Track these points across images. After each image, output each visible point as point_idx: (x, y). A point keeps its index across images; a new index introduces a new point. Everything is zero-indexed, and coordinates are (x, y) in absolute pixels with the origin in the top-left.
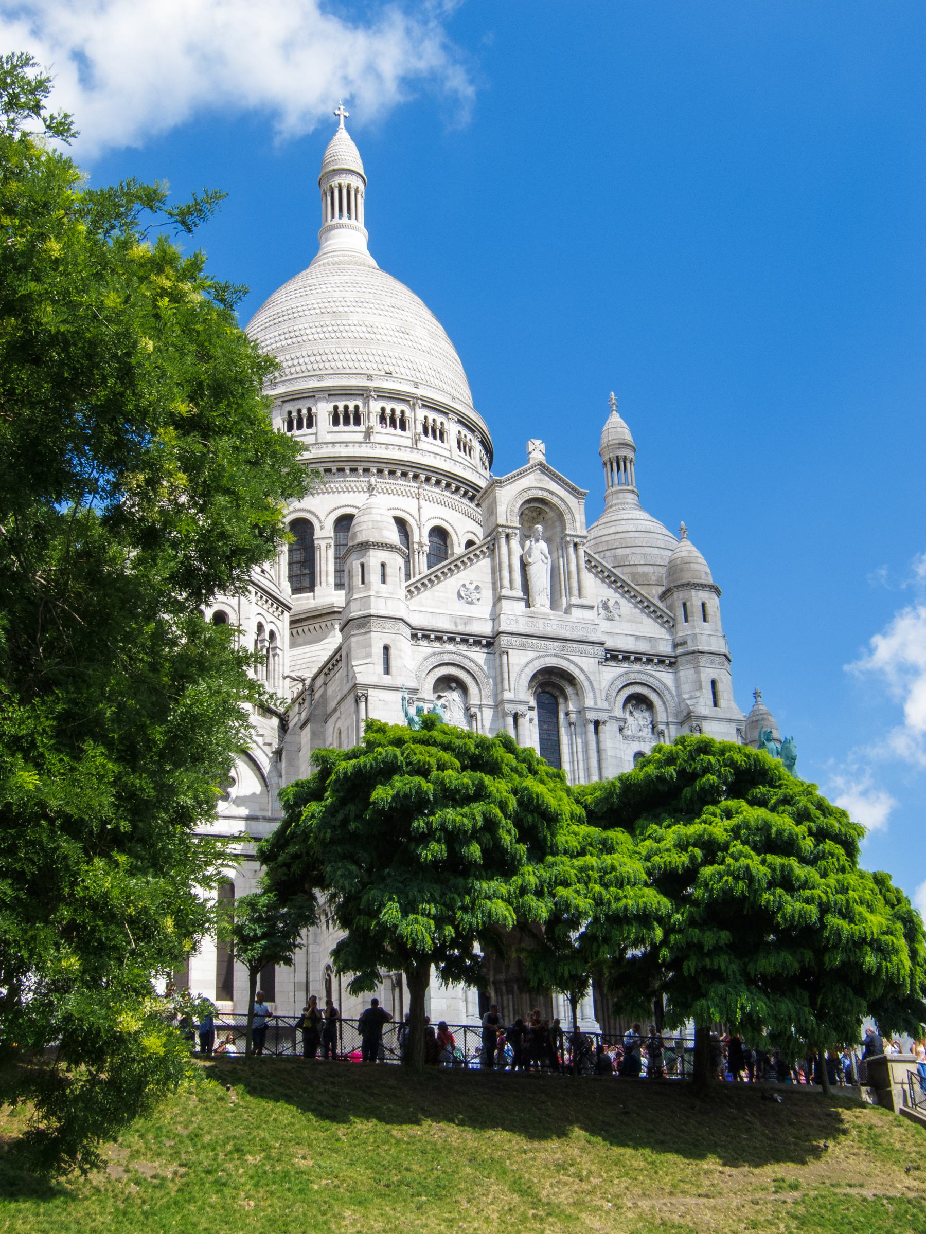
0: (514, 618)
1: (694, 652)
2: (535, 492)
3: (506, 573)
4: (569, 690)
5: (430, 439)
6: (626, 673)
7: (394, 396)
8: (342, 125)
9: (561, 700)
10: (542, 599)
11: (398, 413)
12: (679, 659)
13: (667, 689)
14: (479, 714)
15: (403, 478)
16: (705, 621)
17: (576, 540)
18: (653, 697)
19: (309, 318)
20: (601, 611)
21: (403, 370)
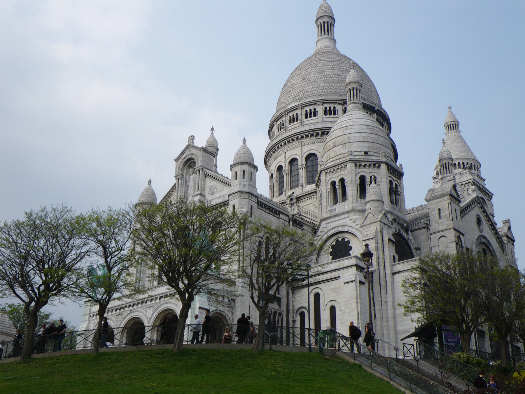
2: (187, 157)
5: (309, 118)
15: (294, 141)
17: (198, 169)
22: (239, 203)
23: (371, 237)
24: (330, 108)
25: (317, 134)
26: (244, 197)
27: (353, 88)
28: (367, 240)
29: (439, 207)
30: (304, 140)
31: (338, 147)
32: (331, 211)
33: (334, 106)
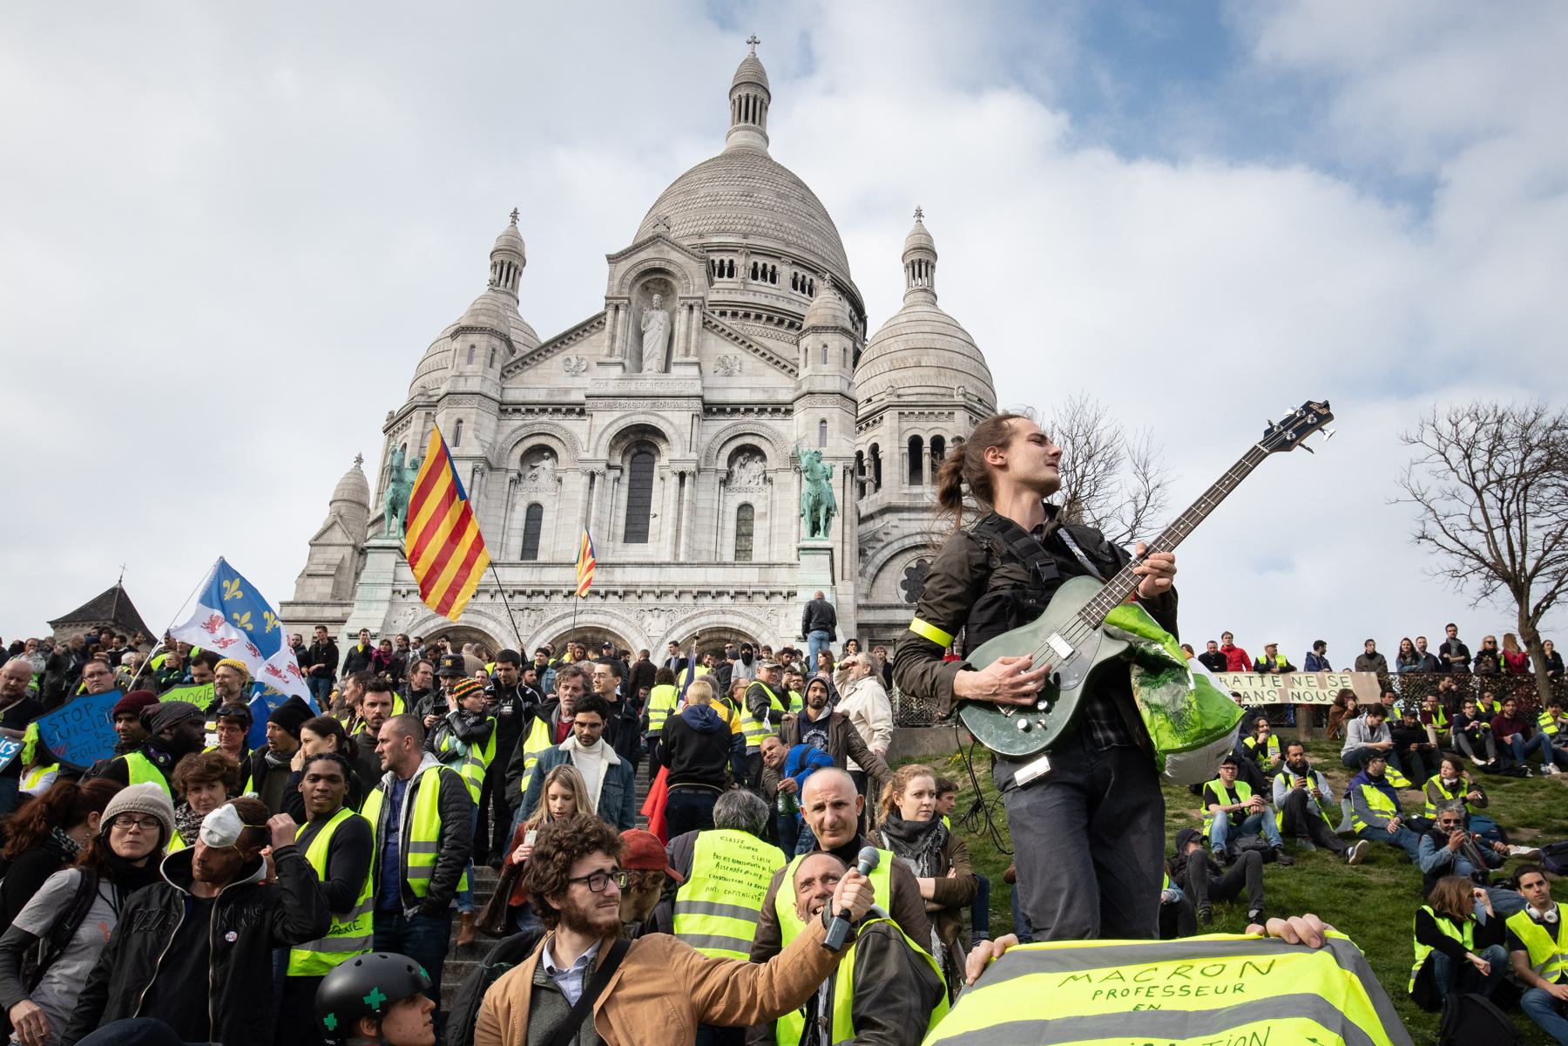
0: (604, 382)
1: (804, 395)
2: (651, 263)
4: (663, 447)
5: (759, 281)
7: (722, 248)
9: (657, 458)
10: (652, 363)
11: (726, 263)
12: (797, 405)
13: (780, 436)
18: (764, 446)
22: (840, 421)
24: (804, 277)
25: (781, 322)
30: (751, 322)
32: (910, 494)
33: (811, 277)
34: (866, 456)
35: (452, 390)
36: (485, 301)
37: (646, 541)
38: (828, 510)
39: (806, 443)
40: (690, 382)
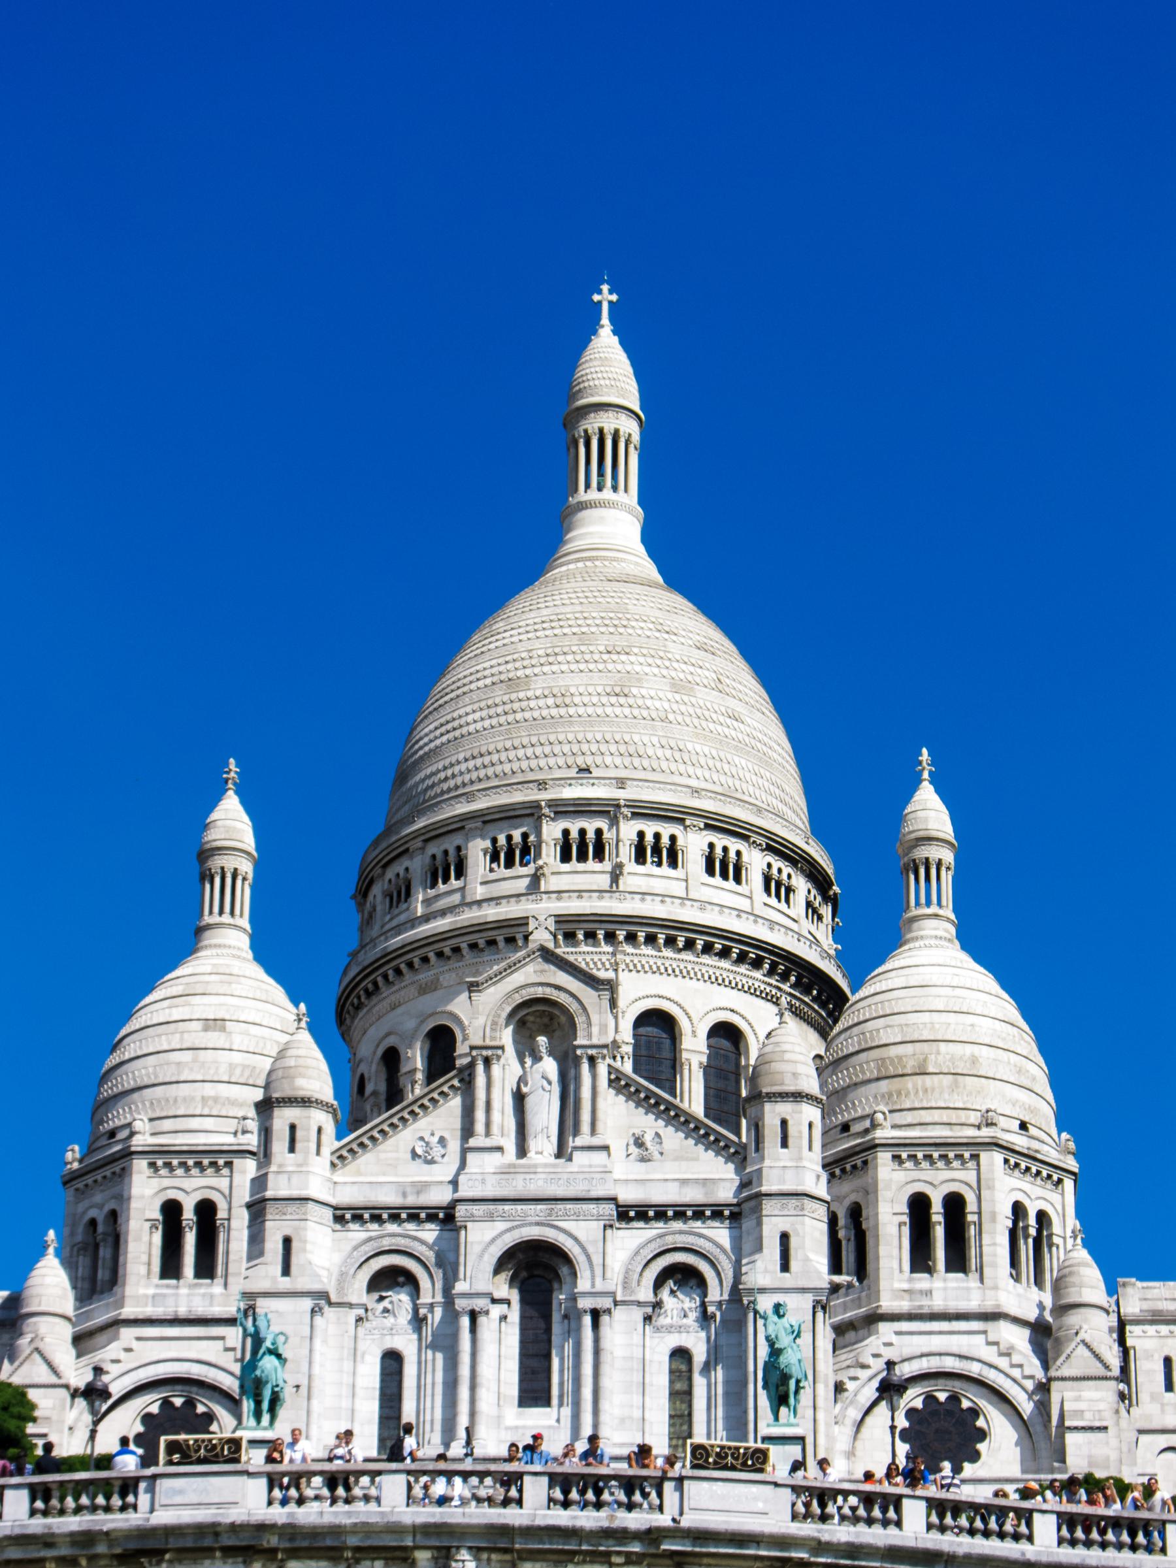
2: (532, 990)
3: (480, 1115)
4: (564, 1271)
5: (649, 868)
6: (661, 1236)
7: (581, 808)
8: (605, 320)
9: (556, 1285)
10: (543, 1145)
11: (591, 835)
12: (746, 1206)
14: (430, 1316)
15: (590, 941)
16: (785, 1144)
17: (590, 1052)
19: (474, 696)
20: (633, 1149)
21: (608, 760)
23: (1097, 1424)
24: (725, 849)
25: (690, 945)
26: (818, 1217)
27: (940, 860)
28: (1083, 1428)
29: (1166, 1352)
31: (935, 1078)
34: (842, 1222)
35: (269, 1194)
36: (301, 1052)
37: (548, 1403)
38: (798, 1382)
39: (759, 1264)
40: (598, 1176)
